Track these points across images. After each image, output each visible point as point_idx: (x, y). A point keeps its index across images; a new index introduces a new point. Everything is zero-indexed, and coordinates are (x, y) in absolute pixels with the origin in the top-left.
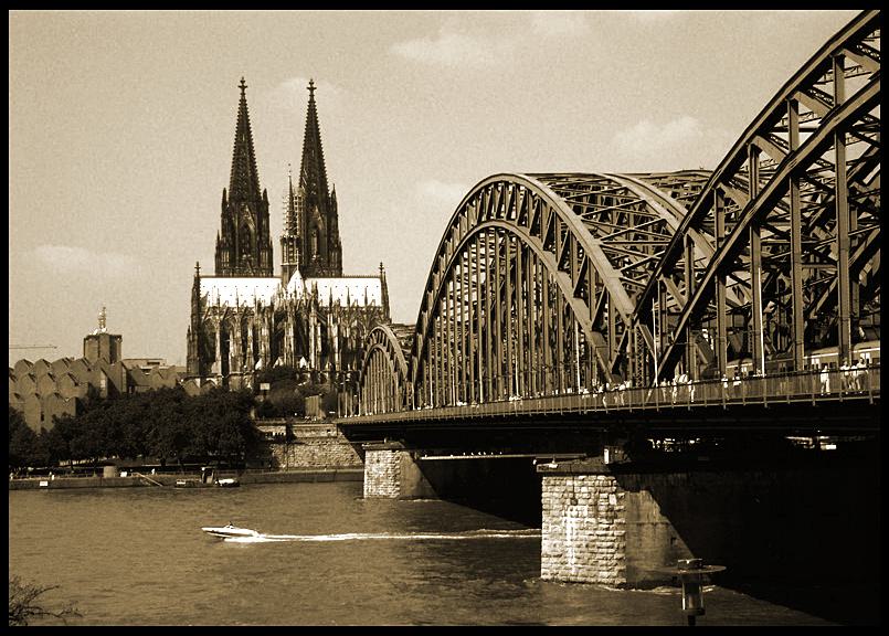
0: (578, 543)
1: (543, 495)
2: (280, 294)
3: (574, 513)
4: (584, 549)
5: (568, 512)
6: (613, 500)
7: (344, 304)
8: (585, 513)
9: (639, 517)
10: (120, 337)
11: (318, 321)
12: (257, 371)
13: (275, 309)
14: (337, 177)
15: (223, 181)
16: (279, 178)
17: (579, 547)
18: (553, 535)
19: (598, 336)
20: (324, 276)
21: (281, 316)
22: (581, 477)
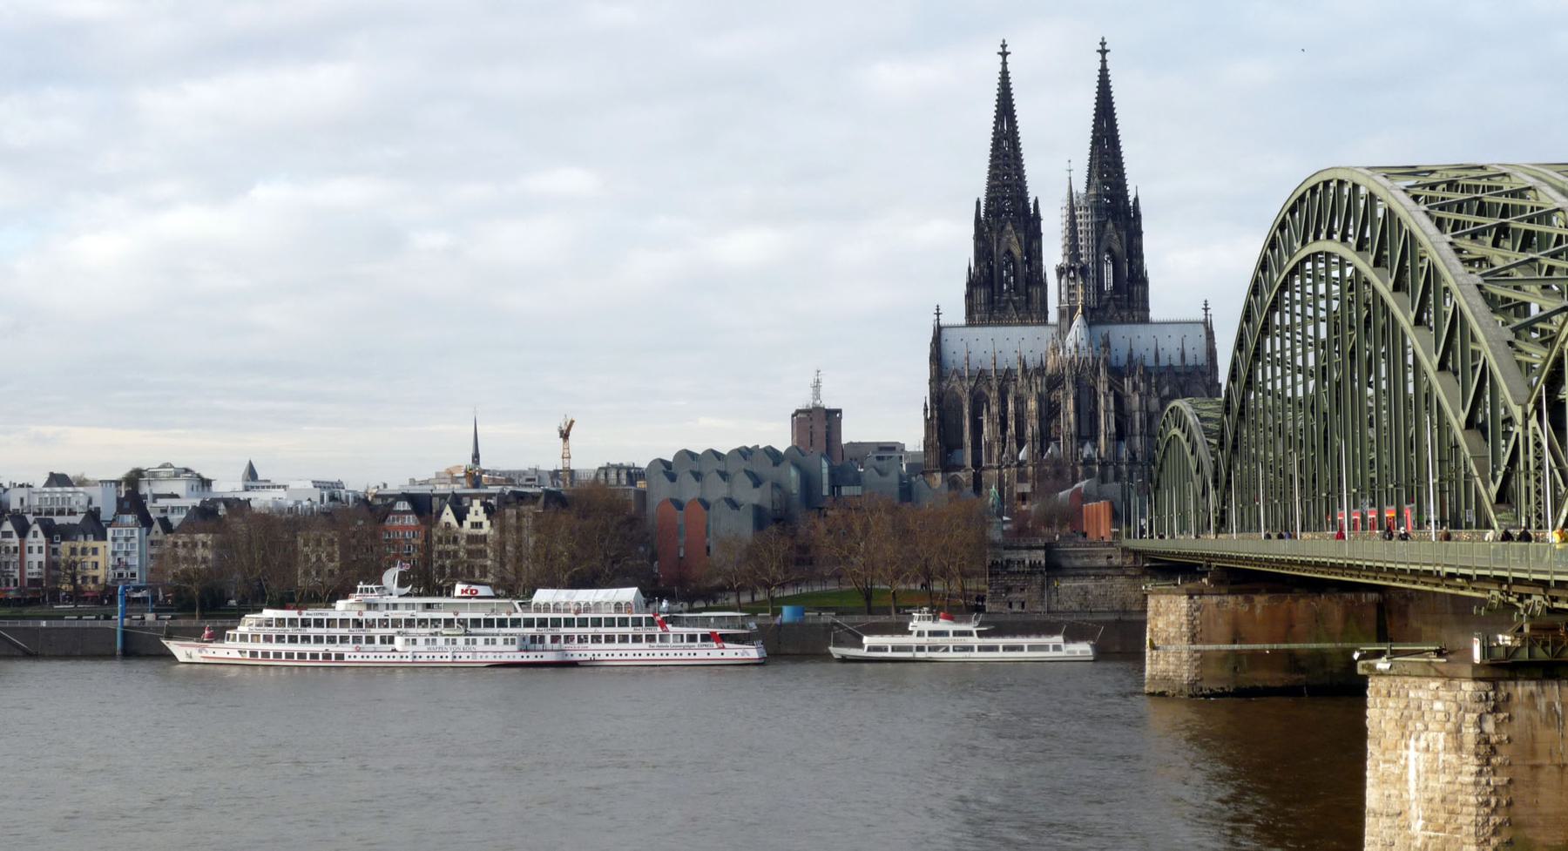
0: (1428, 795)
1: (1368, 712)
2: (1055, 349)
3: (1422, 744)
4: (1437, 803)
5: (1412, 743)
6: (1489, 726)
7: (1150, 362)
8: (1440, 746)
9: (1534, 753)
10: (839, 411)
11: (1110, 389)
12: (1021, 464)
13: (1049, 371)
14: (1138, 181)
15: (975, 182)
16: (1055, 176)
17: (1431, 800)
18: (1383, 781)
19: (1475, 435)
20: (1122, 322)
21: (1055, 382)
22: (1433, 685)
